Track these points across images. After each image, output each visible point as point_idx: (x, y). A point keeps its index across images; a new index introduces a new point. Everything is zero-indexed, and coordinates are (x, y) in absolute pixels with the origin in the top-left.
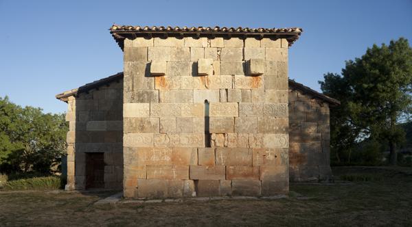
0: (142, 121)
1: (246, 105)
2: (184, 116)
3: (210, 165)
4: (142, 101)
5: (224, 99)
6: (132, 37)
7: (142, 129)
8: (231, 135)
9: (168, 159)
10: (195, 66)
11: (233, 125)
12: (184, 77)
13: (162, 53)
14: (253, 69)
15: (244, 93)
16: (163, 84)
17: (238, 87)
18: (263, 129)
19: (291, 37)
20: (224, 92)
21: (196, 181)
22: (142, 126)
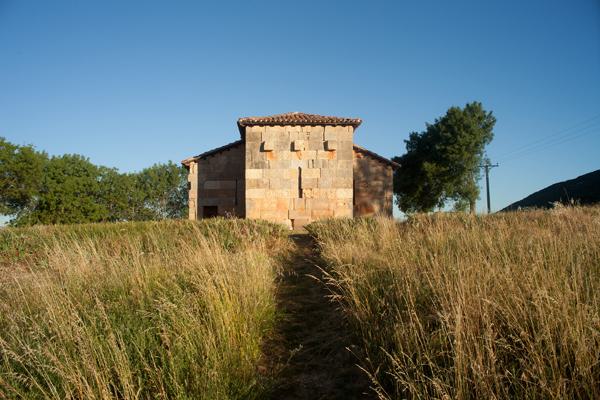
0: (257, 180)
1: (325, 170)
2: (285, 177)
3: (302, 209)
4: (258, 168)
5: (311, 166)
6: (251, 126)
7: (258, 186)
8: (315, 190)
9: (274, 205)
10: (293, 145)
11: (317, 183)
12: (285, 152)
13: (271, 136)
14: (330, 147)
15: (324, 161)
16: (272, 156)
17: (320, 158)
18: (335, 186)
19: (355, 125)
20: (311, 162)
21: (292, 220)
22: (258, 184)
